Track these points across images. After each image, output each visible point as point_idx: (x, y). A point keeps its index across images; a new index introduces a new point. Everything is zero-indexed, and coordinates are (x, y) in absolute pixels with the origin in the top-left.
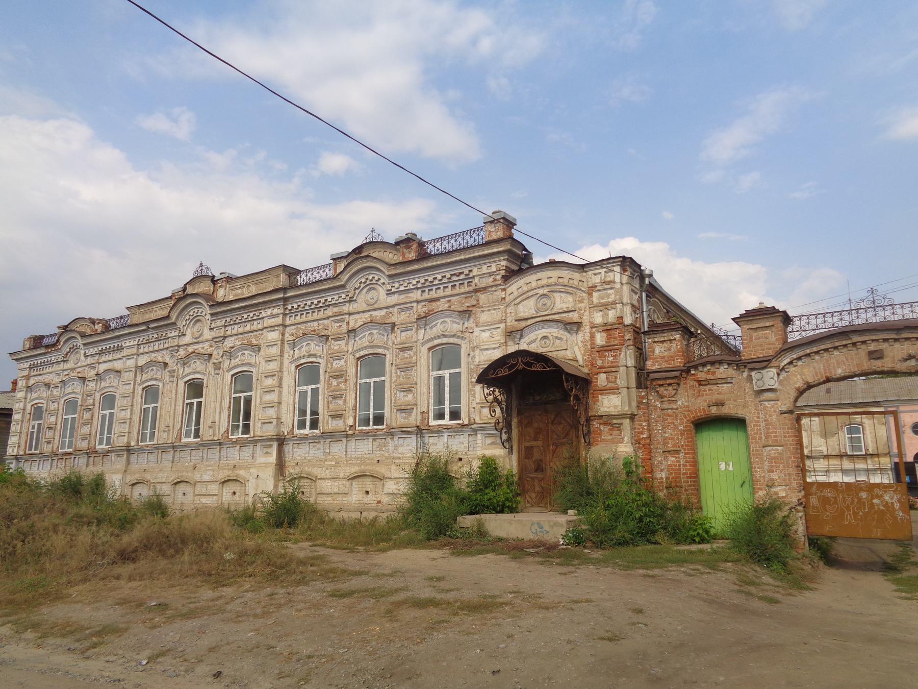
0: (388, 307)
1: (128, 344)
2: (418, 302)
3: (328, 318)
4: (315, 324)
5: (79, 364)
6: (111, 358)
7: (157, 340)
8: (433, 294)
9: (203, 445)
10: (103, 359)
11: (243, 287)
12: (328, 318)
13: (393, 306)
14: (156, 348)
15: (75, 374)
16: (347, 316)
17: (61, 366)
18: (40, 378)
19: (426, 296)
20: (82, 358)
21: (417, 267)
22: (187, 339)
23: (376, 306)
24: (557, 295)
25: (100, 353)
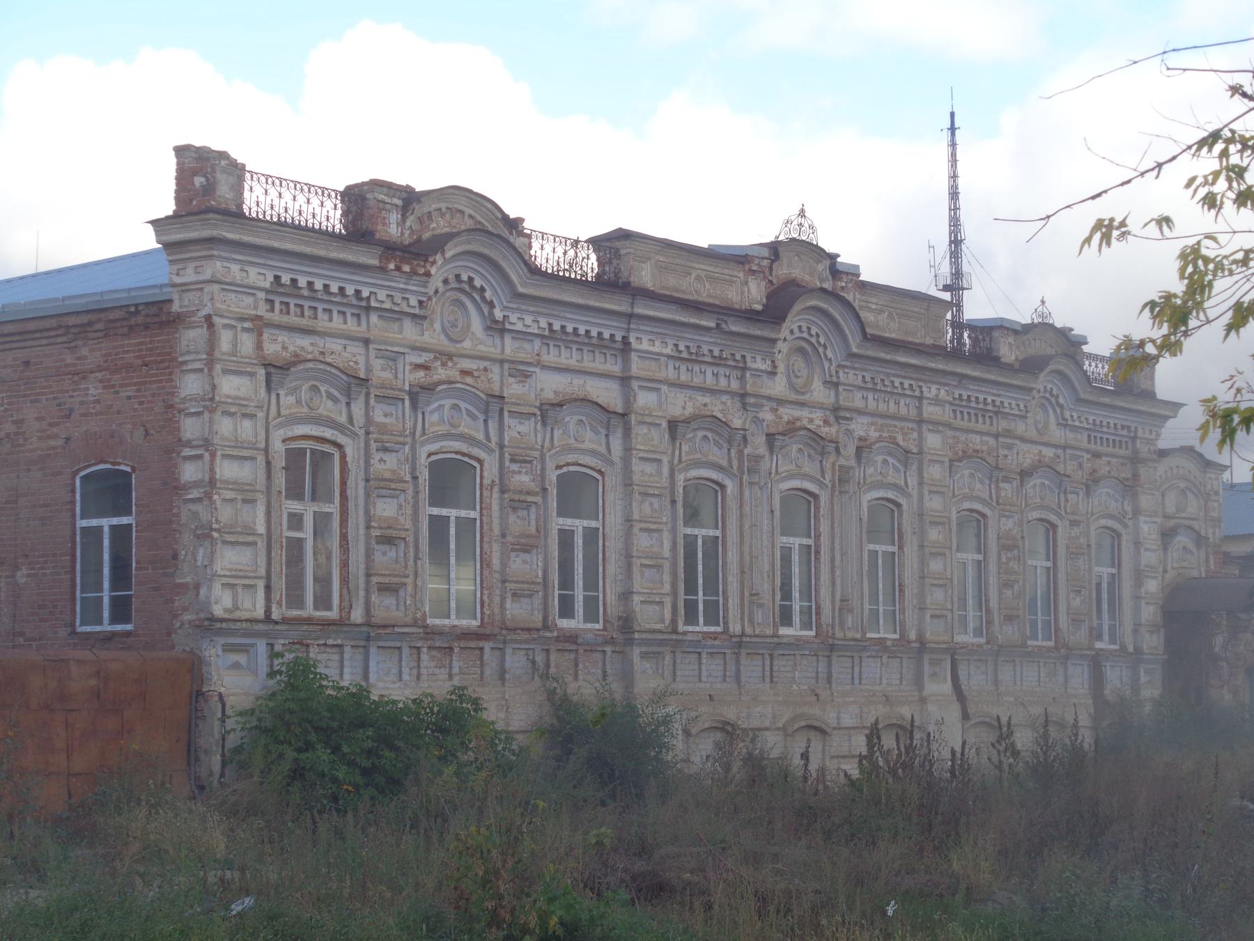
0: (1056, 446)
1: (645, 346)
2: (1088, 451)
3: (996, 436)
4: (977, 438)
5: (467, 344)
6: (573, 362)
7: (718, 361)
8: (1099, 448)
9: (828, 647)
10: (551, 357)
11: (882, 311)
12: (996, 436)
13: (1064, 448)
14: (710, 381)
15: (453, 373)
16: (1017, 442)
17: (409, 331)
18: (304, 342)
19: (1092, 446)
20: (477, 325)
21: (1107, 400)
22: (778, 387)
23: (1045, 439)
24: (1189, 494)
25: (550, 337)
